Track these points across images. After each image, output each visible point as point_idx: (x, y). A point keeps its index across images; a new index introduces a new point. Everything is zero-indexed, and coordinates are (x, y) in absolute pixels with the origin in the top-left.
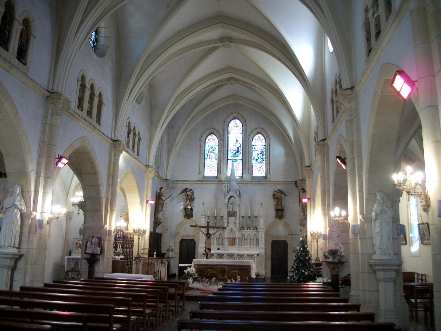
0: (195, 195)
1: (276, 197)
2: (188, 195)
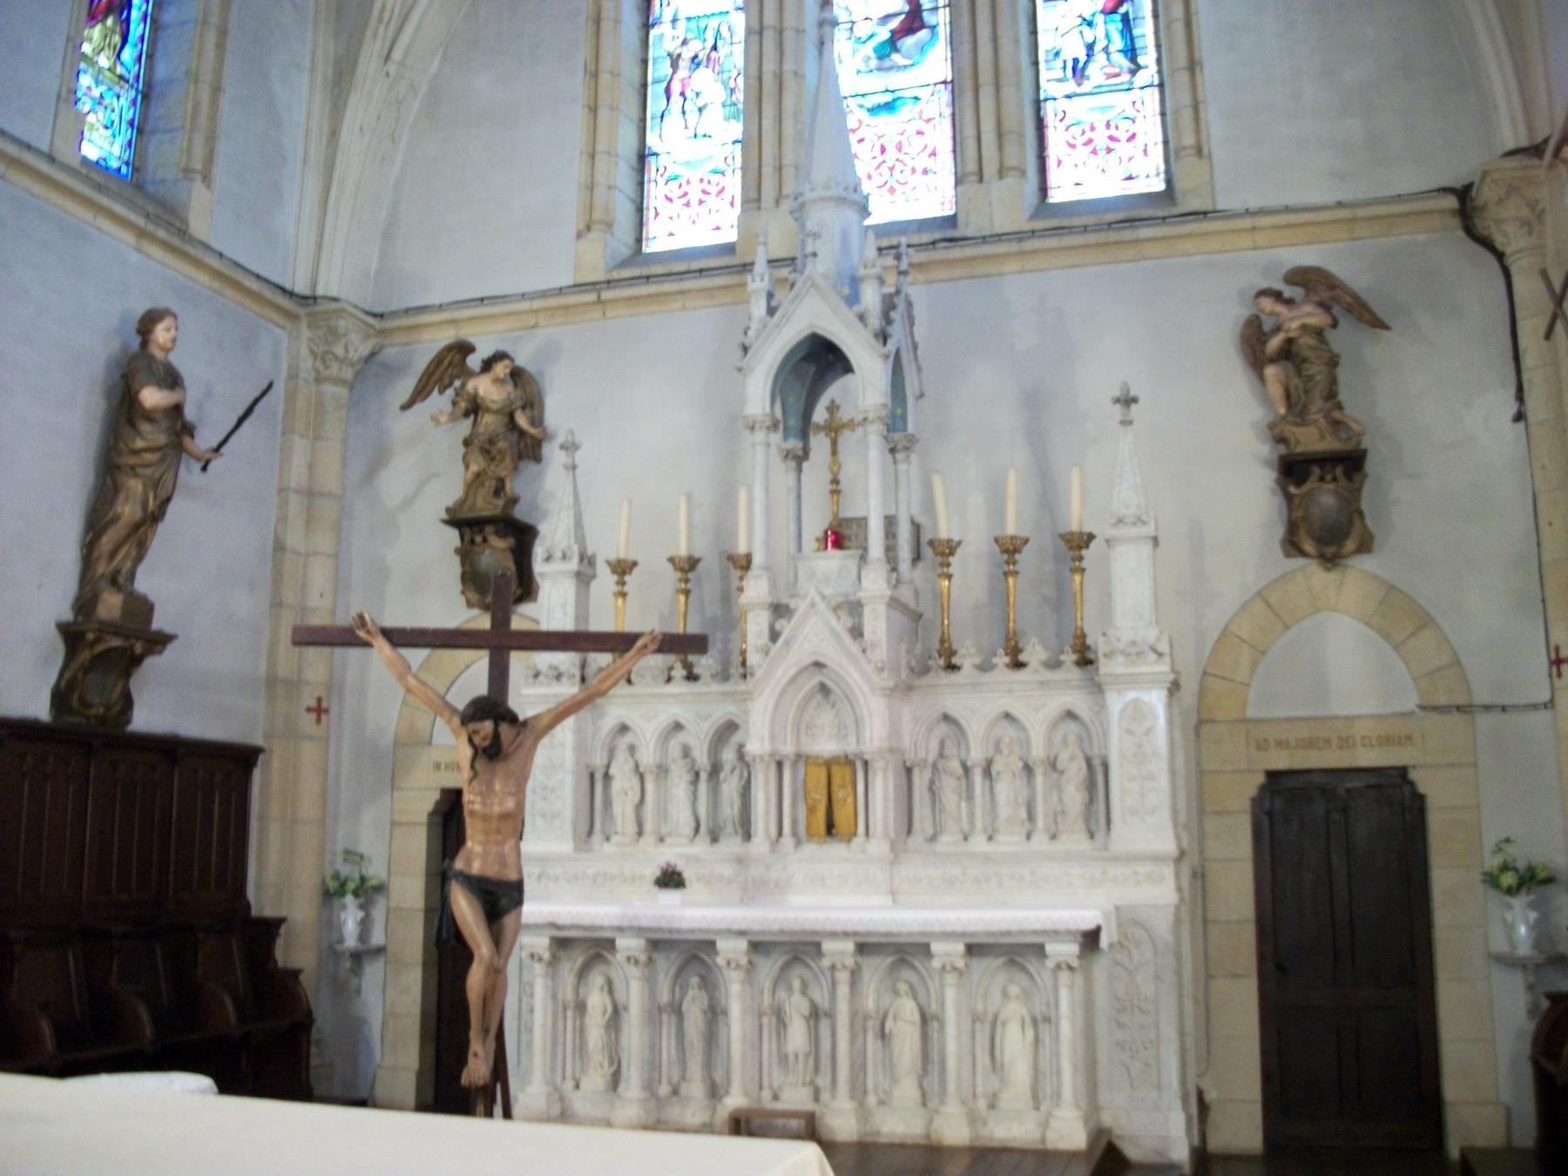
0: (558, 412)
1: (1274, 344)
2: (475, 408)
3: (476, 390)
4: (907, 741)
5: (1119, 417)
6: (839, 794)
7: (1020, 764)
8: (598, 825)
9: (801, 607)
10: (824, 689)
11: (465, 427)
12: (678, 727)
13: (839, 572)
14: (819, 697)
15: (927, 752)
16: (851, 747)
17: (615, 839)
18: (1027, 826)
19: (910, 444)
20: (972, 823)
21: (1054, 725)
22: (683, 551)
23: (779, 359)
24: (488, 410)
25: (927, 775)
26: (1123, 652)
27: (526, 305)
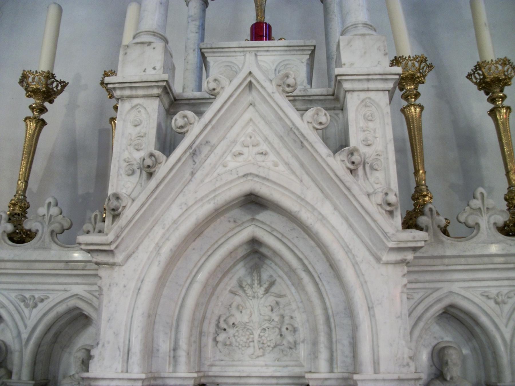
10: (255, 252)
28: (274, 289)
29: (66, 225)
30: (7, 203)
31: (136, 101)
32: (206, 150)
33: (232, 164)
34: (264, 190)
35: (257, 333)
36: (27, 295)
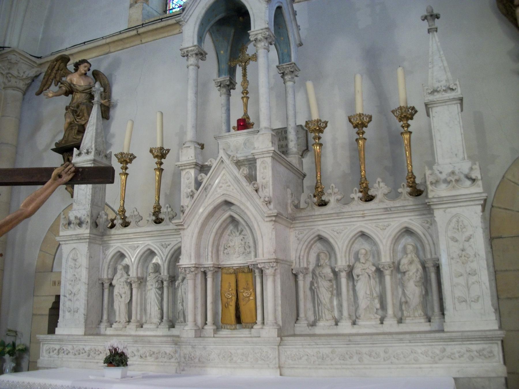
2: (70, 91)
3: (71, 81)
4: (293, 256)
5: (427, 27)
6: (244, 294)
7: (374, 269)
8: (105, 317)
9: (214, 163)
10: (233, 220)
11: (66, 100)
12: (151, 253)
13: (245, 144)
14: (231, 227)
15: (308, 262)
16: (250, 260)
17: (115, 325)
18: (380, 312)
19: (294, 71)
20: (341, 311)
21: (397, 239)
22: (159, 145)
23: (203, 11)
24: (77, 91)
25: (309, 278)
26: (445, 181)
27: (104, 42)
28: (243, 233)
29: (174, 215)
30: (152, 207)
31: (187, 170)
32: (210, 187)
33: (219, 190)
34: (229, 199)
35: (237, 249)
36: (163, 244)
